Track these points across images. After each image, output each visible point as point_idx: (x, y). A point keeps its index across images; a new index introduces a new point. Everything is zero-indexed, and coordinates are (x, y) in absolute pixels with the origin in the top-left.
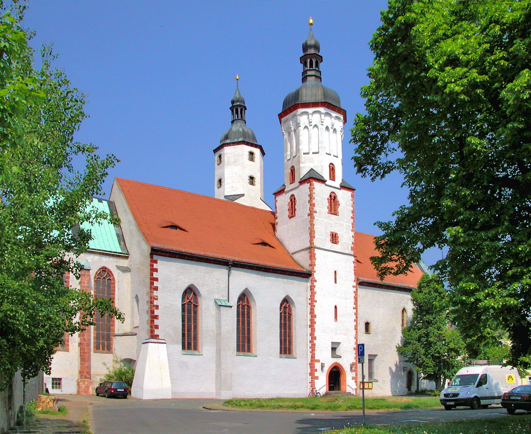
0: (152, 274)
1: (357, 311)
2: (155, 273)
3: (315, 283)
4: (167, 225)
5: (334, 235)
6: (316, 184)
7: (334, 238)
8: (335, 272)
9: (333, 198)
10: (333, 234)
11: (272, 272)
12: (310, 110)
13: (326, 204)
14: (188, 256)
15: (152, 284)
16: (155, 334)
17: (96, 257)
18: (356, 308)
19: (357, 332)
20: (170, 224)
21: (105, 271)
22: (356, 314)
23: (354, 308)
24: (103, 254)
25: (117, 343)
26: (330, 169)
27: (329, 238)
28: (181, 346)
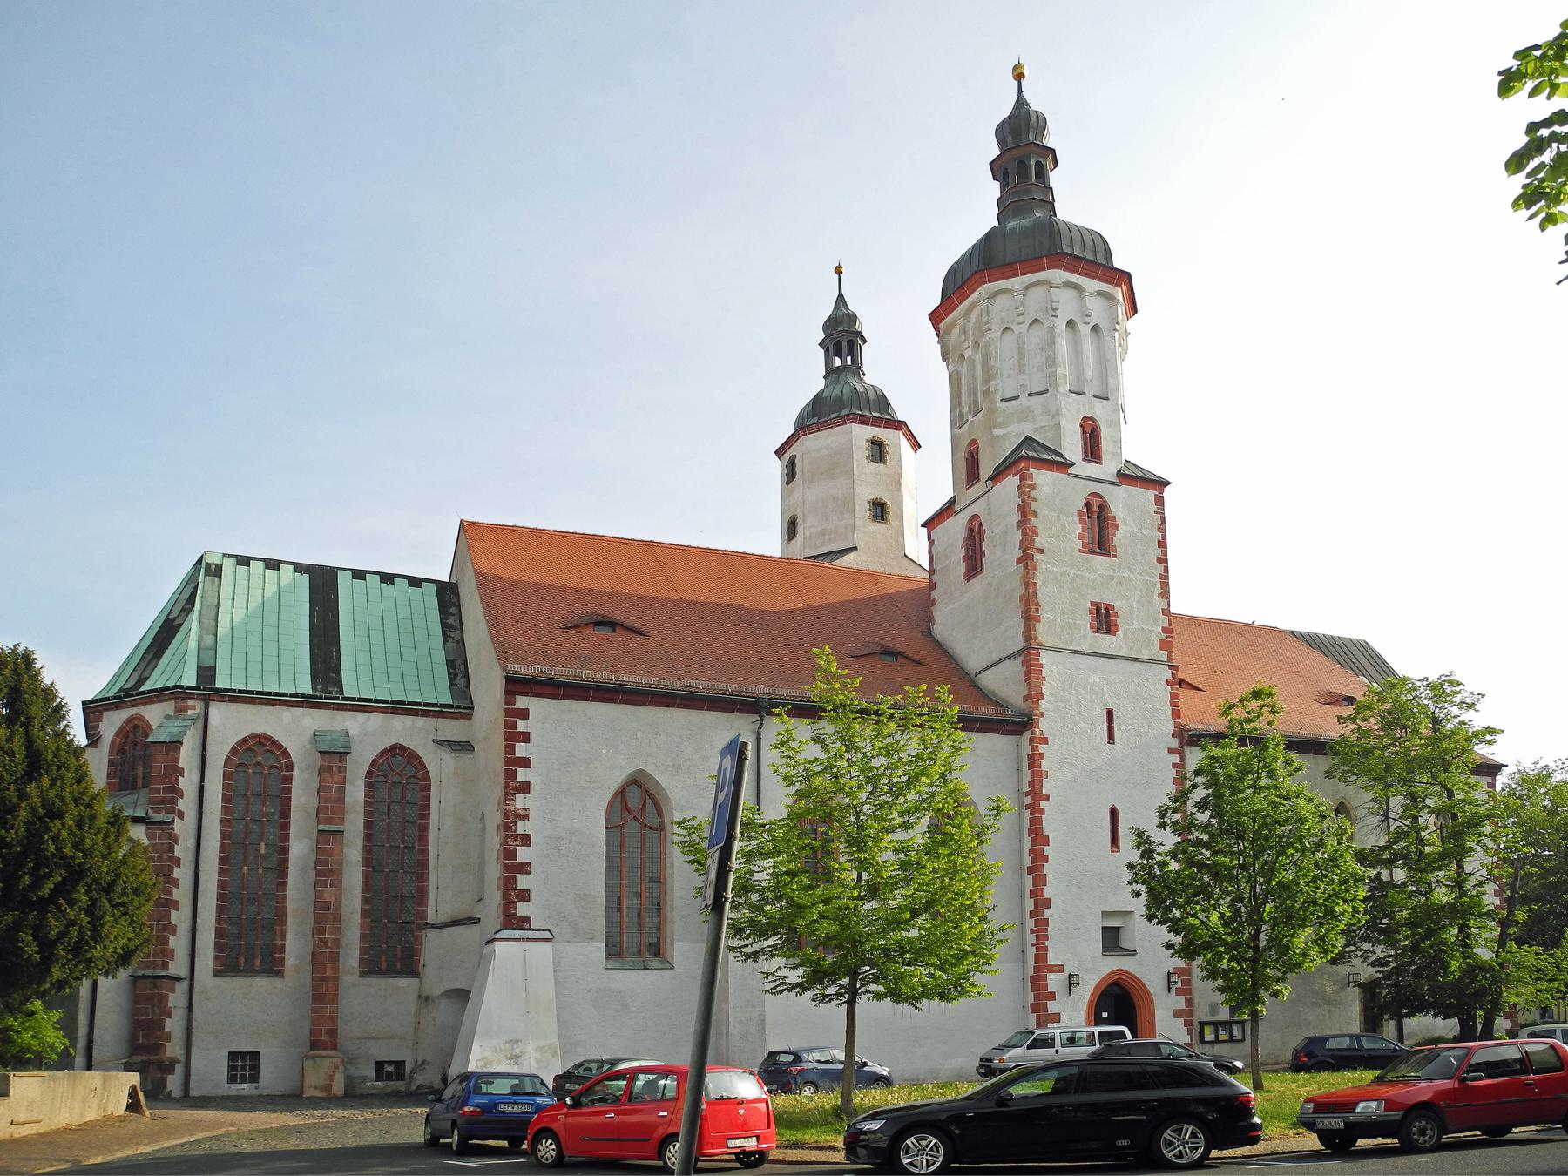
0: (510, 749)
3: (1042, 748)
6: (1043, 479)
8: (1110, 713)
14: (625, 692)
17: (376, 720)
24: (395, 712)
26: (1084, 432)
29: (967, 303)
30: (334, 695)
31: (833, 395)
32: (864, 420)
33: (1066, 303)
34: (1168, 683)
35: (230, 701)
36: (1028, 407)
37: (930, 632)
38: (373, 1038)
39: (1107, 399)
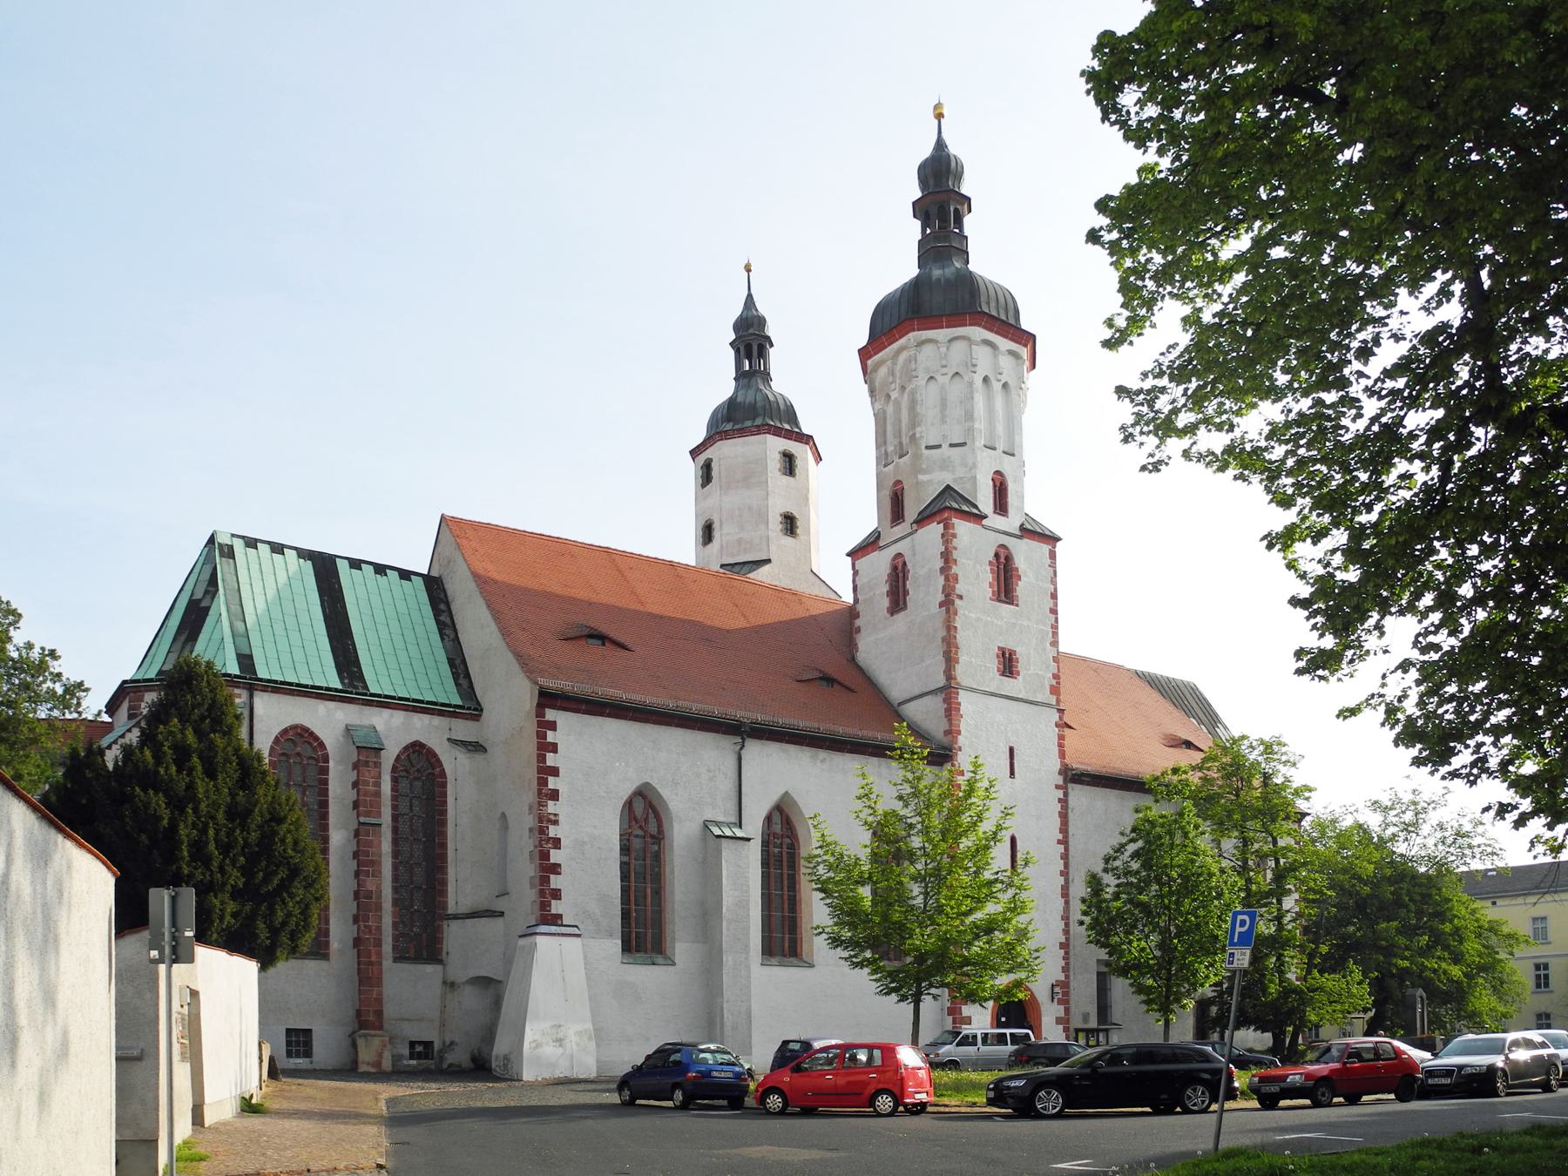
0: (541, 759)
1: (1066, 849)
2: (550, 756)
4: (578, 634)
6: (962, 527)
7: (1008, 664)
8: (1011, 750)
9: (1002, 560)
10: (1004, 654)
11: (851, 751)
14: (636, 710)
15: (543, 782)
16: (553, 911)
17: (398, 717)
18: (1064, 842)
19: (1067, 903)
20: (586, 632)
22: (1065, 857)
23: (1059, 842)
24: (415, 710)
25: (455, 935)
26: (995, 486)
27: (993, 664)
28: (620, 942)
29: (895, 346)
30: (361, 691)
31: (747, 401)
32: (778, 432)
33: (982, 355)
35: (272, 692)
36: (949, 457)
37: (853, 659)
38: (408, 1020)
39: (1013, 455)
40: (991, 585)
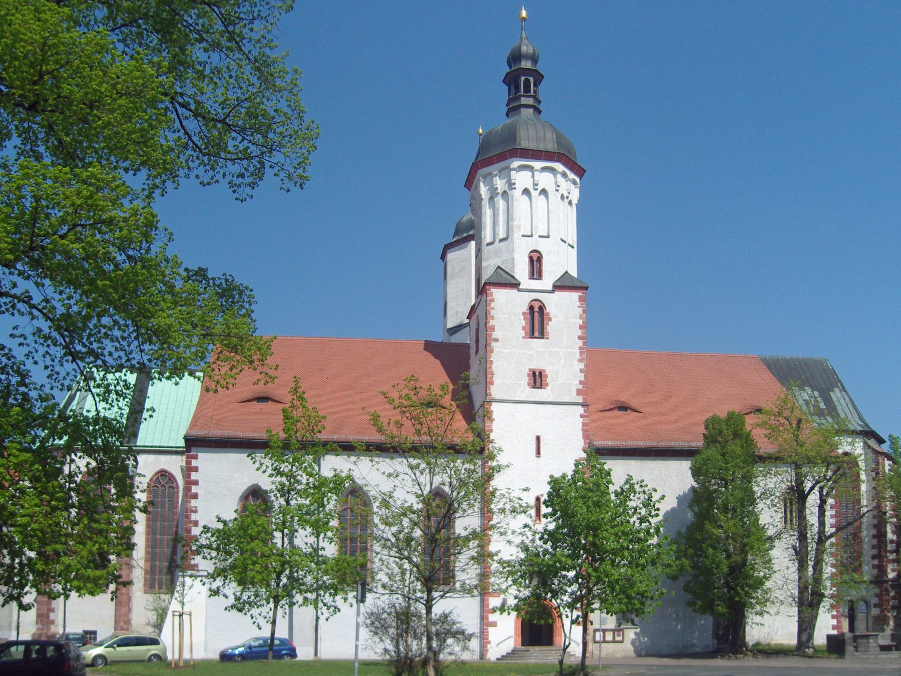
5: (537, 374)
7: (537, 379)
8: (538, 438)
9: (536, 309)
10: (534, 373)
12: (538, 165)
13: (520, 322)
21: (166, 476)
34: (581, 416)
40: (524, 328)
